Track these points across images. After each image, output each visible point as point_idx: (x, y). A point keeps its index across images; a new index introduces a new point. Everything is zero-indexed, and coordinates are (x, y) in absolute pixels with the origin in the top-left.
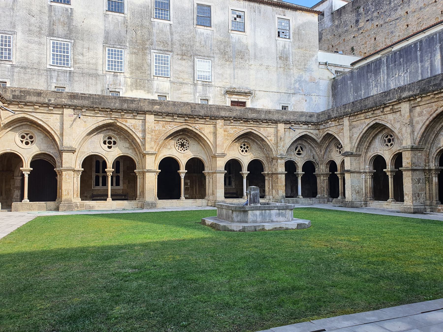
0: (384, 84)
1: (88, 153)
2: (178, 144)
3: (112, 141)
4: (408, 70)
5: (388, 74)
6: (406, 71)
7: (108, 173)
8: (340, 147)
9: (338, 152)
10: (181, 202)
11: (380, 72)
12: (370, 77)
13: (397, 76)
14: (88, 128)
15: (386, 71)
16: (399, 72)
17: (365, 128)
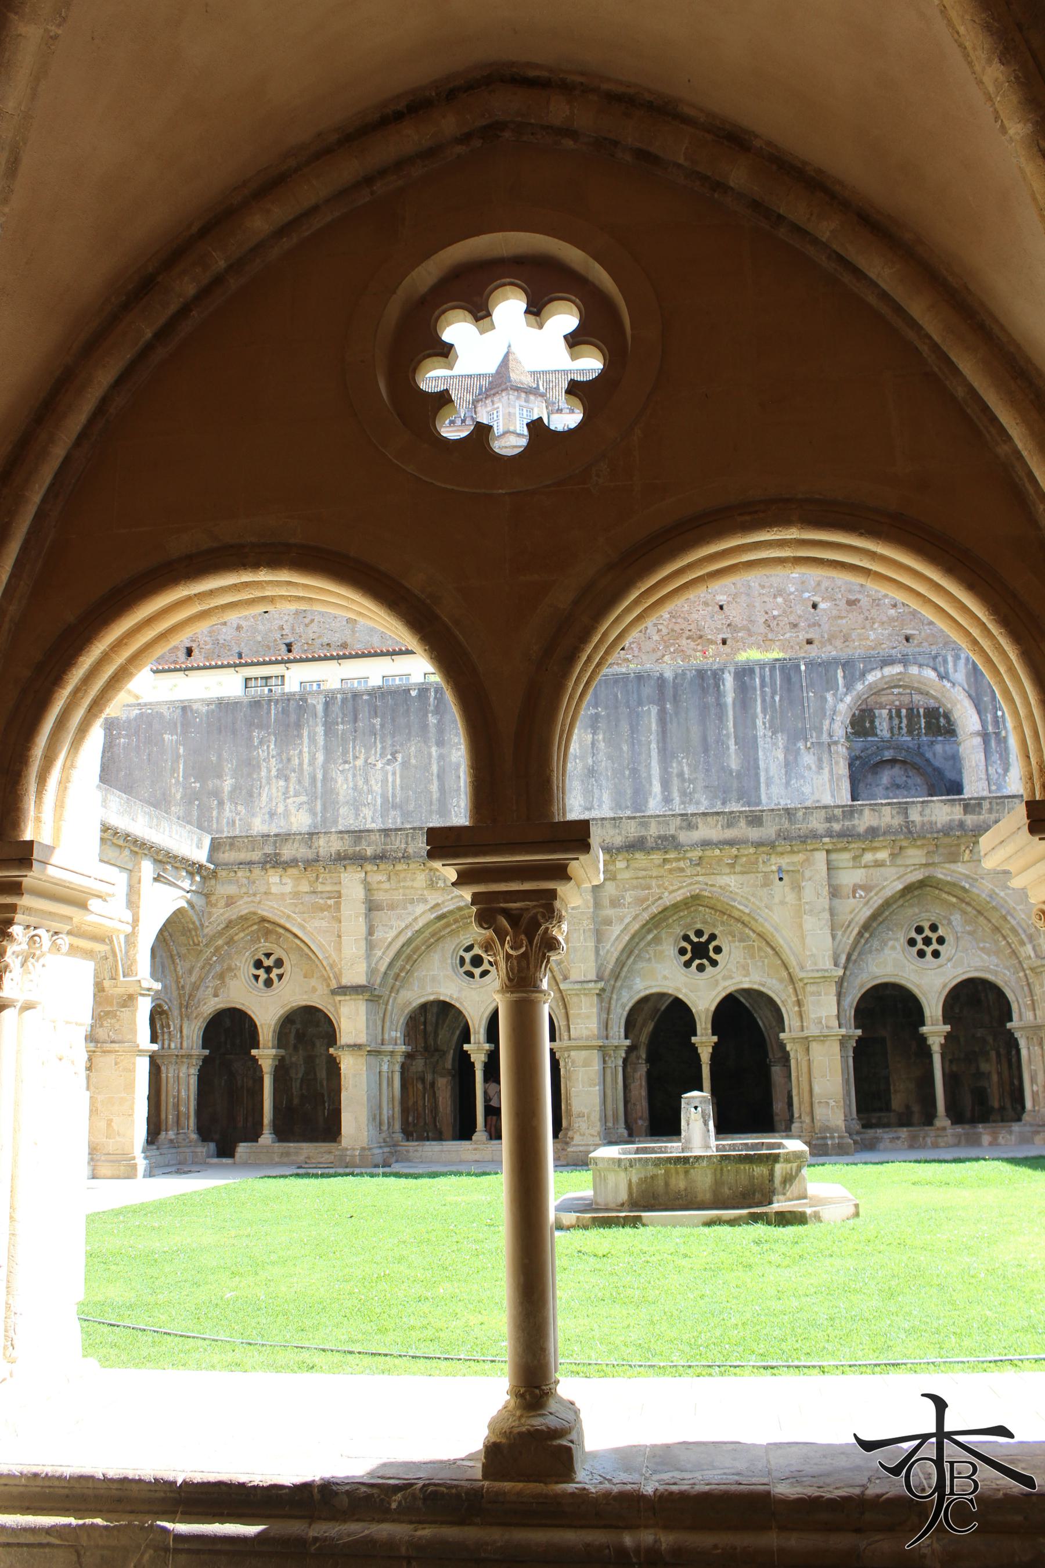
0: (313, 779)
4: (399, 757)
5: (328, 750)
6: (389, 757)
8: (267, 963)
9: (261, 980)
11: (300, 736)
12: (261, 743)
13: (360, 762)
15: (321, 740)
16: (368, 751)
17: (421, 916)
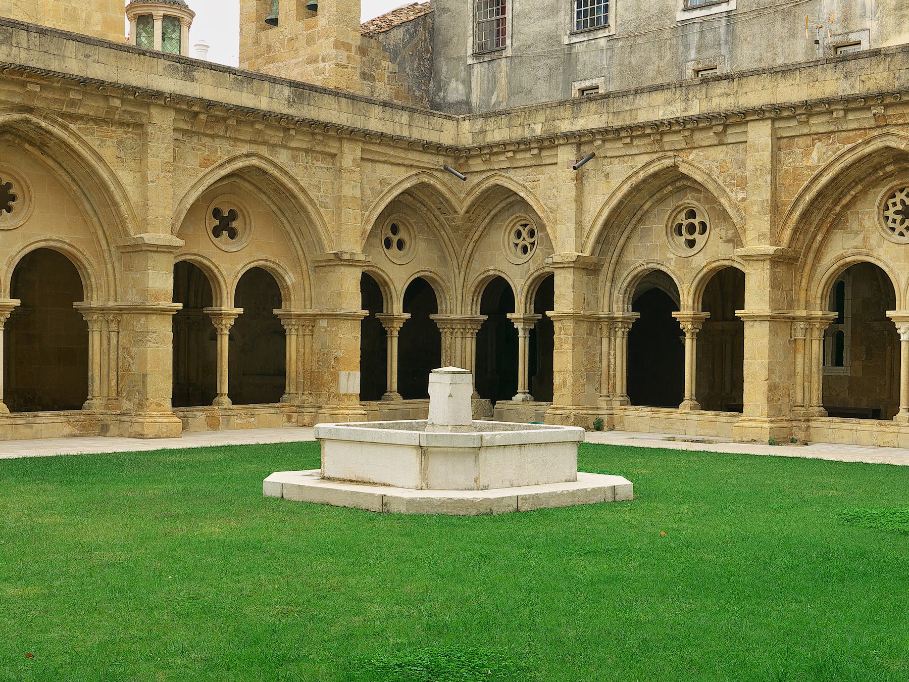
1: (637, 264)
2: (892, 209)
3: (685, 222)
7: (681, 327)
10: (891, 429)
14: (614, 194)
